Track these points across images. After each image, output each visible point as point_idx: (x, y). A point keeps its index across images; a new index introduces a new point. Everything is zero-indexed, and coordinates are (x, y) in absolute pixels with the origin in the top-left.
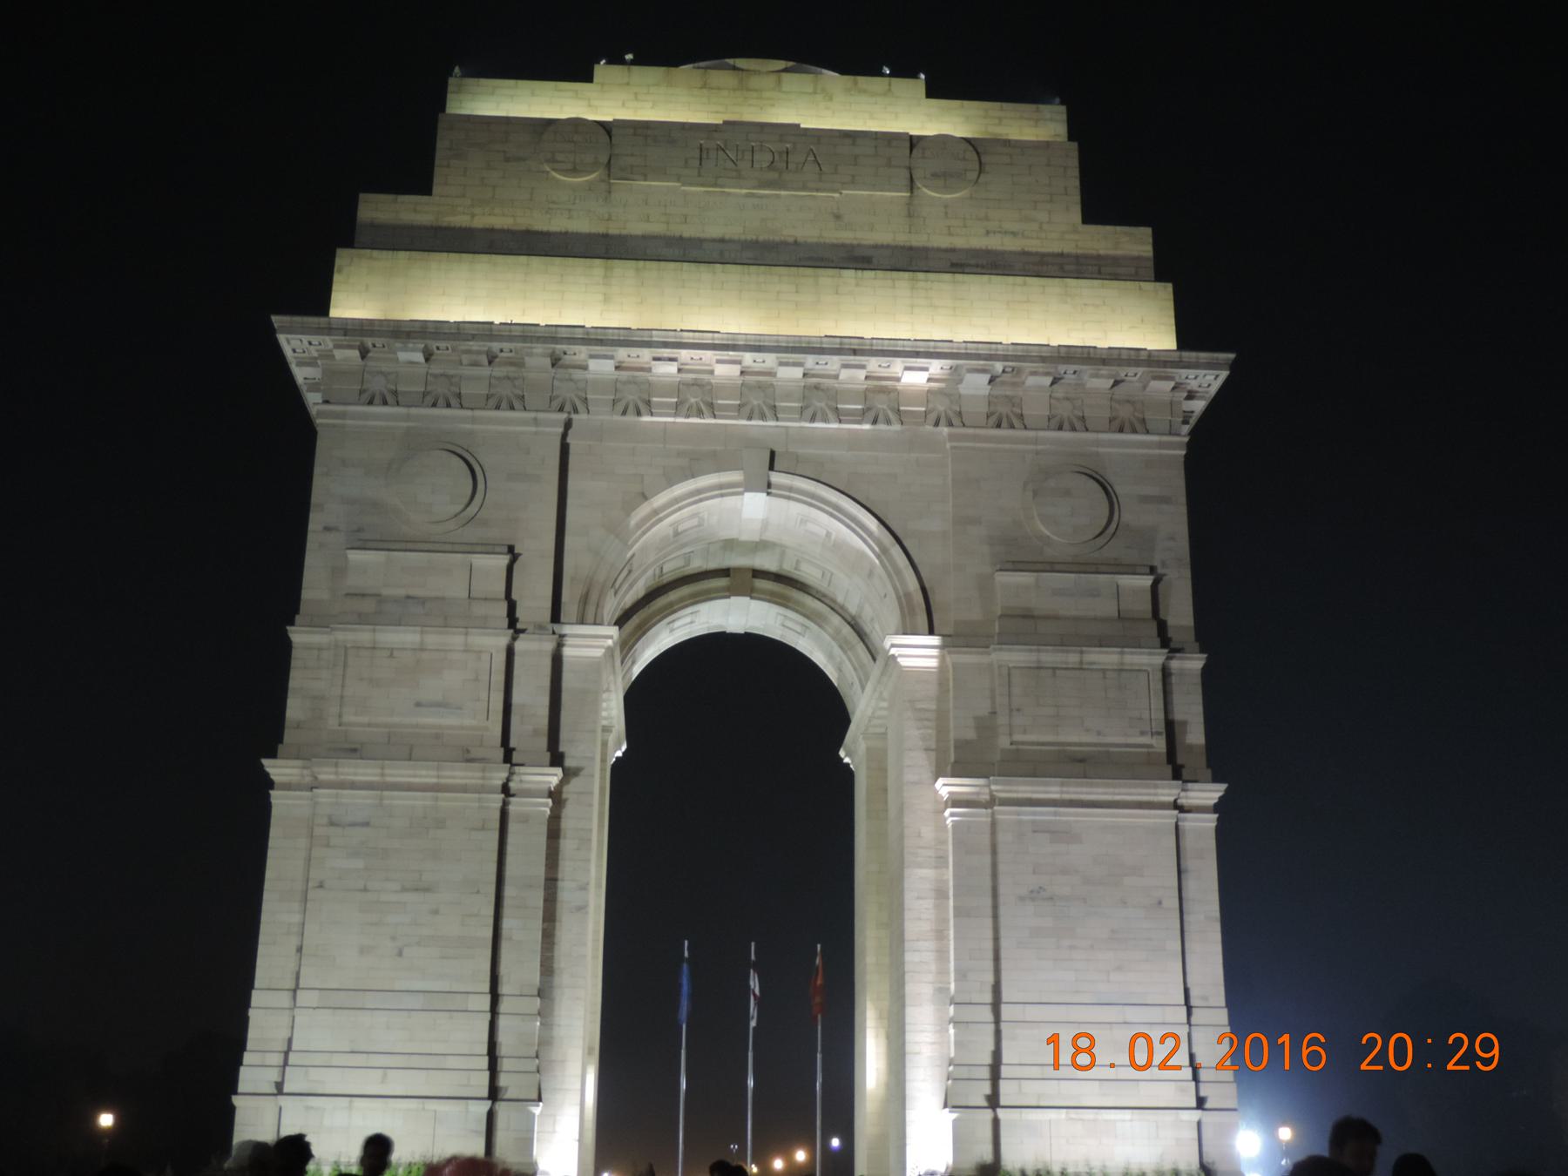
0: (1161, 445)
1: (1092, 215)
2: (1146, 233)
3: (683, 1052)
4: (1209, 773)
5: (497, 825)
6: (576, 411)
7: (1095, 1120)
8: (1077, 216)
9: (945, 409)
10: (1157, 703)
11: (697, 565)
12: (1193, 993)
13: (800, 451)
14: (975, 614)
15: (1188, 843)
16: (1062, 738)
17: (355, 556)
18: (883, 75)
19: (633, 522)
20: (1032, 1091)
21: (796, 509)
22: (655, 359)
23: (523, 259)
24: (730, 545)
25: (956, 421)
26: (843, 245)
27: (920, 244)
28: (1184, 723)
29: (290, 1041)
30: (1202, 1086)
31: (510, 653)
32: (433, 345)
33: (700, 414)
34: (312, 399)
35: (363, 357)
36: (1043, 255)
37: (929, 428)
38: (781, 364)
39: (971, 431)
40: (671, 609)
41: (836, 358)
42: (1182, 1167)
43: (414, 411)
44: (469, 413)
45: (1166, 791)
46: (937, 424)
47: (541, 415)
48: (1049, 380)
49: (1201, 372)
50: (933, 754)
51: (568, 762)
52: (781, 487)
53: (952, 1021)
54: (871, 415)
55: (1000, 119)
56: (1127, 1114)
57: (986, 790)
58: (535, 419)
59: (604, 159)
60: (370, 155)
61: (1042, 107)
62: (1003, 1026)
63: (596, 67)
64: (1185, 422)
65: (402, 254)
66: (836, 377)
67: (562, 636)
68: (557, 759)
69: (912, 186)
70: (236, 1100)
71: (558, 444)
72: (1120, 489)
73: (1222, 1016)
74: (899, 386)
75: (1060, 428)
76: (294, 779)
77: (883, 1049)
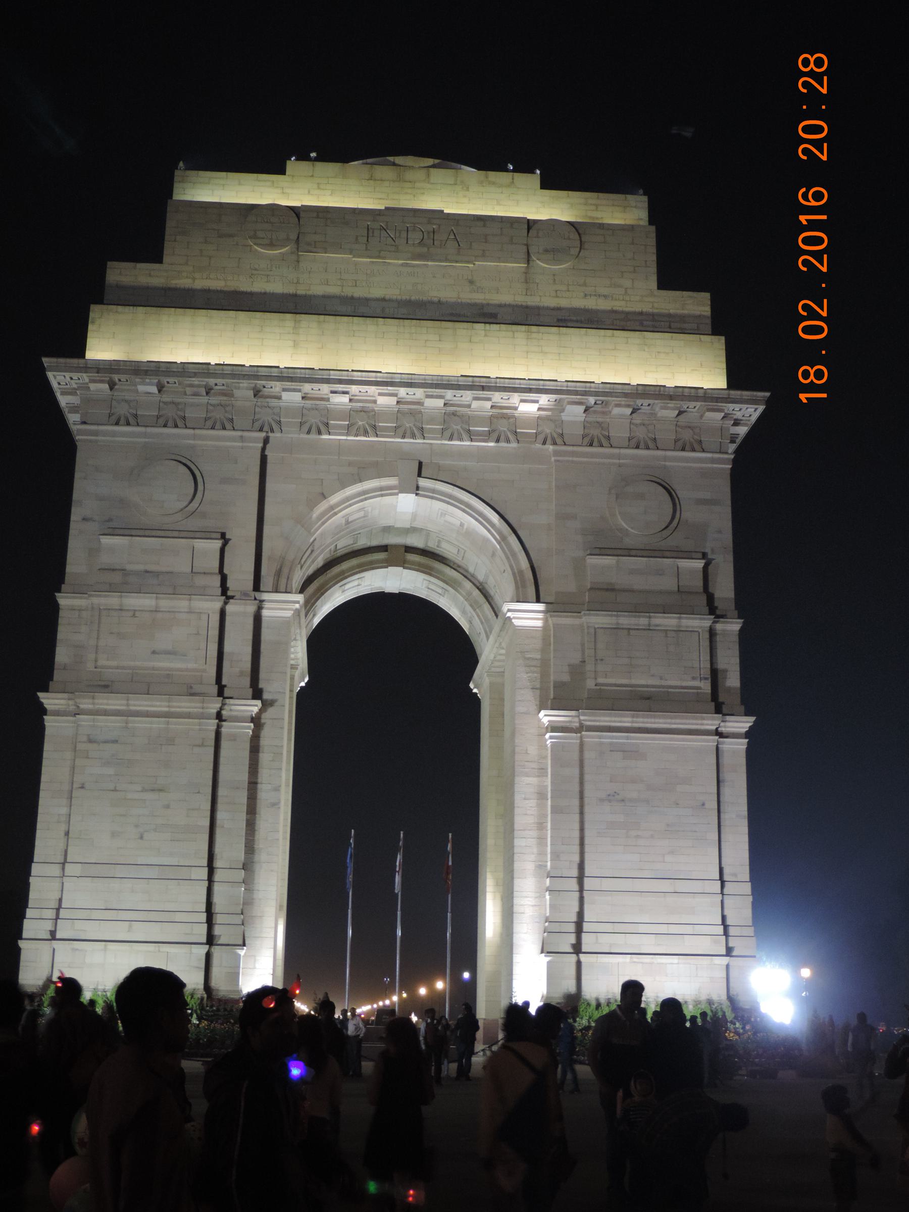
0: (713, 461)
1: (666, 282)
2: (705, 297)
3: (350, 911)
4: (742, 708)
5: (212, 743)
6: (272, 431)
7: (652, 963)
8: (653, 284)
9: (552, 432)
11: (363, 542)
12: (726, 871)
13: (441, 462)
14: (571, 587)
15: (726, 760)
16: (634, 682)
17: (105, 540)
18: (507, 170)
19: (314, 516)
20: (605, 942)
21: (437, 506)
22: (332, 392)
23: (232, 313)
24: (387, 529)
25: (559, 441)
26: (475, 305)
27: (533, 304)
28: (725, 671)
29: (60, 900)
30: (730, 938)
31: (223, 613)
32: (164, 380)
33: (366, 433)
34: (72, 419)
35: (111, 389)
36: (628, 313)
37: (539, 446)
38: (428, 396)
39: (570, 448)
40: (342, 577)
41: (469, 392)
42: (715, 998)
43: (149, 430)
44: (191, 431)
45: (710, 722)
46: (544, 443)
47: (246, 434)
48: (629, 411)
49: (744, 406)
50: (538, 692)
51: (266, 696)
53: (548, 889)
54: (495, 436)
55: (597, 205)
56: (675, 959)
57: (576, 719)
58: (242, 437)
59: (293, 236)
60: (116, 234)
61: (629, 196)
62: (585, 894)
63: (288, 162)
64: (733, 441)
65: (141, 309)
66: (469, 406)
67: (262, 601)
68: (257, 694)
69: (528, 262)
70: (22, 944)
72: (682, 493)
74: (516, 413)
75: (637, 447)
76: (62, 708)
77: (498, 908)
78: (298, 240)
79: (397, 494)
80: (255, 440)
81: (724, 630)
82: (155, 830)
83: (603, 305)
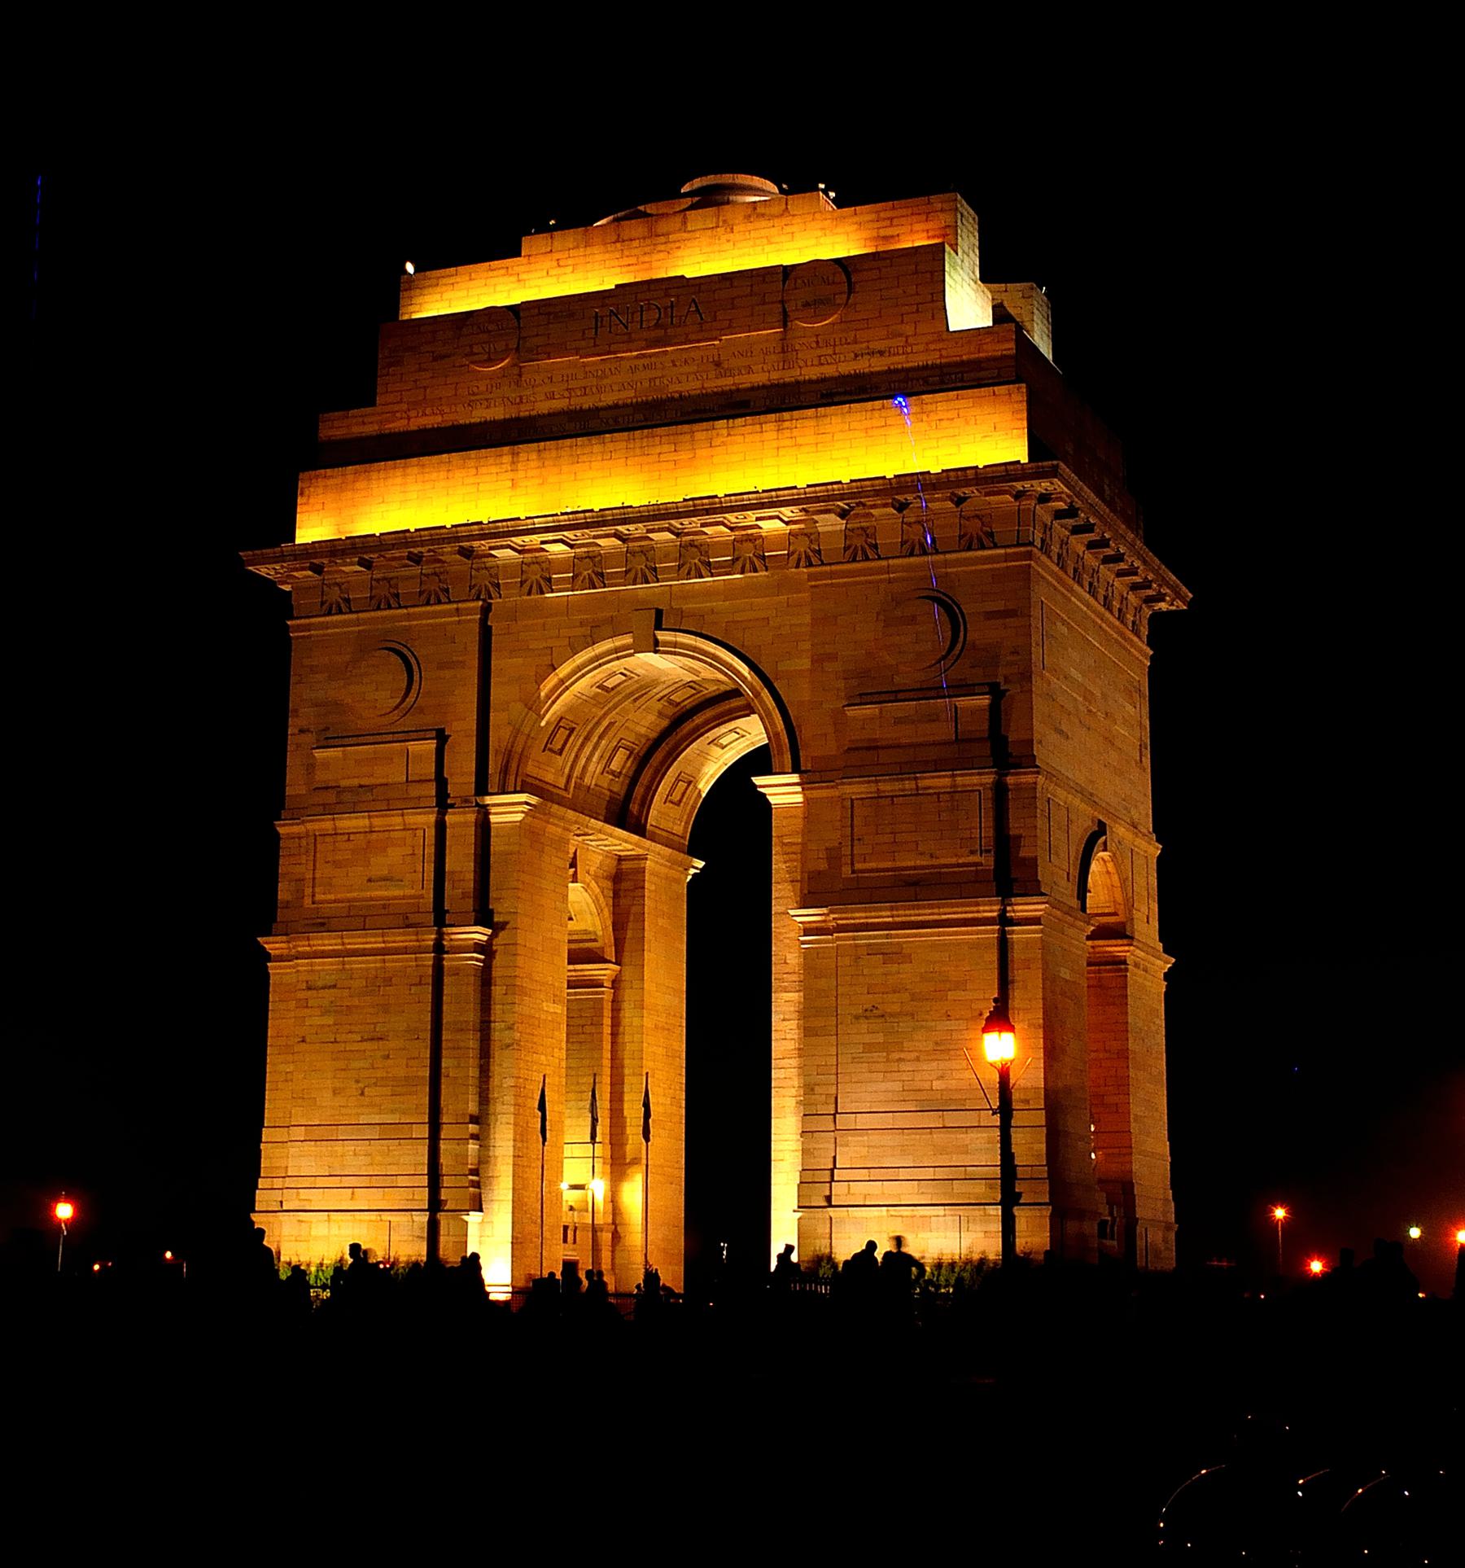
9: (807, 550)
10: (988, 823)
15: (1017, 954)
17: (319, 754)
26: (723, 393)
31: (441, 827)
52: (666, 644)
56: (940, 1210)
59: (513, 344)
69: (785, 321)
70: (254, 1217)
71: (476, 628)
73: (1040, 1118)
78: (517, 349)
79: (631, 655)
80: (470, 611)
81: (1017, 785)
82: (375, 1084)
83: (878, 364)
